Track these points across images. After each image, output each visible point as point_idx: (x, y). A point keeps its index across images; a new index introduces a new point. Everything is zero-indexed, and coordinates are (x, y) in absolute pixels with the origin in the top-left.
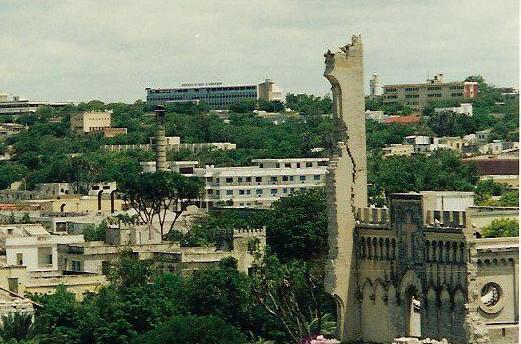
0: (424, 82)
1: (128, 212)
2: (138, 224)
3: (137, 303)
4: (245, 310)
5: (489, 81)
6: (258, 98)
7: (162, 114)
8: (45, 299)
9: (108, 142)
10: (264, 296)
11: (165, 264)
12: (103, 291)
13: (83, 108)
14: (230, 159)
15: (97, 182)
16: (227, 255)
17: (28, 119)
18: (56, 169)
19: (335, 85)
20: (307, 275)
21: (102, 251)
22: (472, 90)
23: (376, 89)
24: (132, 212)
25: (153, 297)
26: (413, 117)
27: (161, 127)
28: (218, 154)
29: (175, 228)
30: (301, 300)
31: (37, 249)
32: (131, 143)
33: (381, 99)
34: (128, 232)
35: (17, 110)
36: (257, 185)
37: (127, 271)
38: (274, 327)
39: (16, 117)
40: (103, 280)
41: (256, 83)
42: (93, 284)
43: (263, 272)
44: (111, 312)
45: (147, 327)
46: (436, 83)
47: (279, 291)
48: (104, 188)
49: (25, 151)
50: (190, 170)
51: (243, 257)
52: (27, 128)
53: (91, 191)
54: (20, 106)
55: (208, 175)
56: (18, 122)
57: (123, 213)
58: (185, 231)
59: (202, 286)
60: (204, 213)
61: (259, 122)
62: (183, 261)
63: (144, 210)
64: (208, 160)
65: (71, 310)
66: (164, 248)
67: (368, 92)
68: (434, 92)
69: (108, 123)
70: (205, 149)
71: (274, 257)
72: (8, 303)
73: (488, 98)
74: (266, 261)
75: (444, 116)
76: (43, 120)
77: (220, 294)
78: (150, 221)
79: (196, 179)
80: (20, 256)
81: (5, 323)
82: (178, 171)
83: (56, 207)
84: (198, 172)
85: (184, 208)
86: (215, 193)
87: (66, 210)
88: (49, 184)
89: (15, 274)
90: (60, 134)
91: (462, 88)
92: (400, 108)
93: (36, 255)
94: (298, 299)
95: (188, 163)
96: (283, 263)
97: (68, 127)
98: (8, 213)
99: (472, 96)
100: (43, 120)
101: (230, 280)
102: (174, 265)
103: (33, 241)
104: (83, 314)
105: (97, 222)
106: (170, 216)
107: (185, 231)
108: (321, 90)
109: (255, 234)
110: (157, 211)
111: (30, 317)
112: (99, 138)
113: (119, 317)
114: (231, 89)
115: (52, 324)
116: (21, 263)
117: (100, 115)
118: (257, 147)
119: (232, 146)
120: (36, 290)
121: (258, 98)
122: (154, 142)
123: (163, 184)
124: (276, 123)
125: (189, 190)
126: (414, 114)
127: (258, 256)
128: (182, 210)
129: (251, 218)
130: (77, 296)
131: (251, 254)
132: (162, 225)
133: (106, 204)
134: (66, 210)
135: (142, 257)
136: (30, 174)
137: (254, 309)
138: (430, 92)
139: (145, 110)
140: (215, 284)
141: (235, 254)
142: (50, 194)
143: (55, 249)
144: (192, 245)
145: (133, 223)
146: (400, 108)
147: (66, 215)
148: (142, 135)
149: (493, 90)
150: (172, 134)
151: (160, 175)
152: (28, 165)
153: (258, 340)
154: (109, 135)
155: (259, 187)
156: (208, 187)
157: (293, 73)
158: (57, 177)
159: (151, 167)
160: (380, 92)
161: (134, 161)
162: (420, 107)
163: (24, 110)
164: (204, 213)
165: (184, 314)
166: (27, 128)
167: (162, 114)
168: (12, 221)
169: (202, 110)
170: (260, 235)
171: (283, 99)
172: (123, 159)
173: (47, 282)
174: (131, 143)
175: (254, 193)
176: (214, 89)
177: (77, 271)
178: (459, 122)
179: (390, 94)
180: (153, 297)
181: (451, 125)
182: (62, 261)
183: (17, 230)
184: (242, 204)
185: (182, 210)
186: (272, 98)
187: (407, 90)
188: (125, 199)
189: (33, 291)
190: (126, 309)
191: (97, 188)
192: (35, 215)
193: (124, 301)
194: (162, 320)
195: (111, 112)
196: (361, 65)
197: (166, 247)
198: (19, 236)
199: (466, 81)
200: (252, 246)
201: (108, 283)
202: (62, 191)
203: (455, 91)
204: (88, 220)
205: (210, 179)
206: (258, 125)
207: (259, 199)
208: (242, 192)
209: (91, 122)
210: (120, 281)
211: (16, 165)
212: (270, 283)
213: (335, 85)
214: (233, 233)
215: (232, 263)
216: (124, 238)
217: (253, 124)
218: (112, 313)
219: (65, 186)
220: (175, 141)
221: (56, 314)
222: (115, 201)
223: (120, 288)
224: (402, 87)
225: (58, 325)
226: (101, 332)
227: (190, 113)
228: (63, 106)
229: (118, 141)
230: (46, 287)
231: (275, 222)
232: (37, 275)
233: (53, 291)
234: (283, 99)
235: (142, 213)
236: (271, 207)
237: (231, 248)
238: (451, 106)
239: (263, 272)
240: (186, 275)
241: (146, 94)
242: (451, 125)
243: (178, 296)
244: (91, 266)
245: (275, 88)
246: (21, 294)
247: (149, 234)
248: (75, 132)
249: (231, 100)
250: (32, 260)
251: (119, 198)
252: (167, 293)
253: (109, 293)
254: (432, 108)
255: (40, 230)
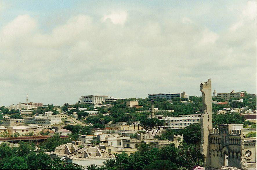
0: (229, 92)
1: (143, 130)
2: (146, 133)
3: (146, 156)
4: (177, 158)
5: (248, 92)
6: (181, 97)
7: (153, 102)
8: (119, 155)
9: (137, 110)
10: (182, 154)
11: (154, 145)
12: (136, 153)
13: (130, 100)
14: (173, 115)
15: (134, 121)
16: (172, 143)
17: (114, 103)
18: (122, 118)
19: (203, 93)
20: (195, 148)
21: (136, 141)
22: (243, 95)
23: (215, 94)
24: (144, 130)
25: (150, 155)
26: (226, 103)
27: (153, 105)
28: (169, 113)
29: (157, 135)
30: (193, 155)
31: (116, 141)
32: (144, 110)
33: (216, 97)
34: (143, 136)
35: (111, 101)
36: (180, 122)
37: (143, 147)
38: (185, 163)
39: (110, 103)
40: (136, 150)
41: (180, 93)
42: (133, 151)
43: (182, 147)
44: (138, 159)
45: (148, 163)
46: (232, 93)
47: (187, 153)
48: (136, 123)
49: (113, 112)
50: (161, 118)
51: (176, 143)
52: (114, 106)
53: (132, 124)
54: (112, 99)
55: (166, 119)
56: (111, 104)
57: (142, 130)
58: (160, 136)
59: (164, 151)
60: (165, 130)
61: (181, 104)
62: (159, 144)
63: (148, 129)
64: (166, 115)
65: (126, 158)
66: (153, 141)
67: (213, 95)
68: (232, 95)
69: (137, 104)
70: (165, 112)
71: (185, 143)
72: (108, 156)
73: (248, 97)
74: (183, 144)
75: (235, 102)
76: (118, 103)
77: (170, 154)
78: (149, 133)
79: (163, 121)
80: (112, 143)
81: (107, 162)
82: (158, 118)
83: (122, 129)
84: (163, 119)
85: (159, 129)
86: (168, 125)
87: (125, 130)
88: (120, 122)
89: (110, 148)
90: (123, 107)
91: (240, 94)
92: (222, 100)
93: (116, 142)
94: (192, 155)
95: (160, 116)
96: (188, 145)
97: (126, 105)
98: (108, 130)
99: (243, 96)
100: (118, 103)
101: (173, 150)
102: (156, 145)
103: (116, 138)
104: (130, 159)
105: (134, 133)
106: (155, 131)
107: (160, 136)
108: (199, 95)
109: (180, 136)
110: (151, 130)
111: (115, 160)
112: (135, 109)
113: (140, 161)
114: (173, 94)
115: (121, 162)
116: (112, 145)
117: (135, 102)
118: (180, 111)
119: (173, 111)
120: (116, 153)
121: (181, 97)
122: (151, 110)
123: (153, 122)
124: (186, 104)
125: (161, 124)
126: (226, 102)
127: (181, 143)
128: (159, 129)
129: (179, 132)
130: (128, 155)
131: (179, 142)
132: (153, 134)
133: (137, 128)
134: (125, 130)
135: (147, 143)
136: (115, 119)
137: (180, 158)
138: (231, 95)
139: (148, 101)
140: (168, 151)
141: (174, 142)
142: (120, 125)
143: (122, 141)
144: (162, 140)
145: (144, 133)
146: (222, 100)
147: (125, 131)
148: (147, 108)
149: (249, 95)
150: (156, 108)
151: (152, 119)
152: (114, 116)
153: (181, 167)
154: (137, 108)
155: (181, 123)
156: (166, 123)
157: (191, 90)
158: (122, 120)
159: (150, 117)
160: (216, 95)
161: (144, 115)
162: (228, 100)
163: (113, 100)
164: (165, 130)
165: (159, 159)
166: (114, 106)
167: (153, 101)
168: (109, 133)
169: (165, 100)
170: (181, 137)
171: (188, 97)
172: (142, 115)
173: (119, 150)
174: (144, 110)
175: (179, 124)
176: (168, 94)
177: (128, 147)
178: (239, 104)
179: (219, 96)
180: (150, 155)
181: (237, 105)
182: (124, 144)
183: (111, 135)
184: (176, 128)
185: (159, 129)
186: (185, 97)
187: (224, 95)
188: (142, 126)
189: (115, 153)
190: (142, 158)
191: (134, 123)
192: (116, 131)
193: (142, 156)
194: (153, 161)
195: (138, 101)
196: (211, 88)
197: (154, 140)
198: (111, 137)
199: (241, 92)
200: (179, 140)
201: (137, 151)
202: (124, 124)
203: (238, 95)
204: (131, 132)
205: (167, 120)
206: (181, 105)
207: (181, 126)
208: (176, 124)
209: (132, 104)
210: (141, 150)
211: (111, 116)
212: (184, 151)
213: (203, 93)
214: (173, 136)
215: (173, 145)
216: (142, 138)
217: (179, 105)
218: (139, 159)
219: (125, 123)
220: (157, 109)
221: (122, 159)
222: (139, 127)
223: (141, 152)
224: (222, 94)
225: (123, 163)
226: (135, 165)
227: (161, 101)
228: (124, 99)
229: (140, 110)
230: (119, 152)
231: (186, 133)
232: (117, 148)
233: (121, 153)
234: (188, 97)
235: (147, 130)
236: (184, 129)
237: (173, 140)
238: (237, 99)
239: (182, 147)
240: (160, 148)
241: (148, 96)
242: (237, 105)
243: (157, 154)
244: (132, 146)
245: (186, 94)
246: (112, 154)
247: (149, 136)
248: (128, 107)
249: (173, 98)
250: (115, 144)
251: (140, 126)
252: (155, 154)
253: (138, 154)
254: (232, 100)
255: (117, 135)
